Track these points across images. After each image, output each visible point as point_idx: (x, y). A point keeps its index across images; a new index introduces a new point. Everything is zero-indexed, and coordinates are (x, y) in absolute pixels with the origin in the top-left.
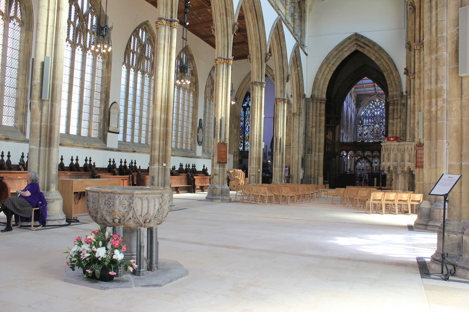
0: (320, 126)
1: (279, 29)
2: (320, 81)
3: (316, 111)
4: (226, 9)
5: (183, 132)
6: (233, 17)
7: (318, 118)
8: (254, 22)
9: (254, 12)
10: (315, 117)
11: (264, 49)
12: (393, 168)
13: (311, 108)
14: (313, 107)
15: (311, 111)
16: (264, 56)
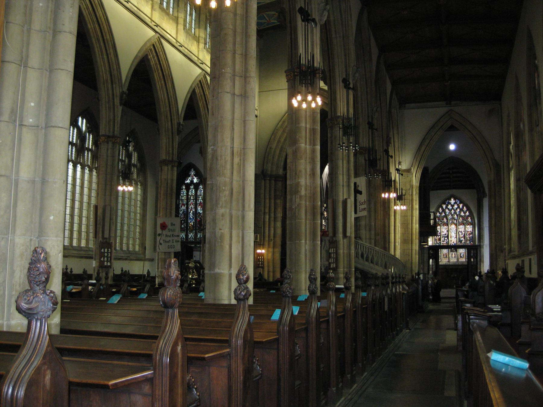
0: (275, 212)
1: (204, 88)
2: (275, 152)
3: (270, 192)
4: (111, 75)
5: (82, 224)
6: (120, 85)
7: (273, 201)
8: (160, 83)
9: (160, 71)
10: (267, 201)
11: (175, 117)
12: (325, 269)
13: (263, 188)
14: (265, 186)
15: (263, 191)
16: (176, 126)
